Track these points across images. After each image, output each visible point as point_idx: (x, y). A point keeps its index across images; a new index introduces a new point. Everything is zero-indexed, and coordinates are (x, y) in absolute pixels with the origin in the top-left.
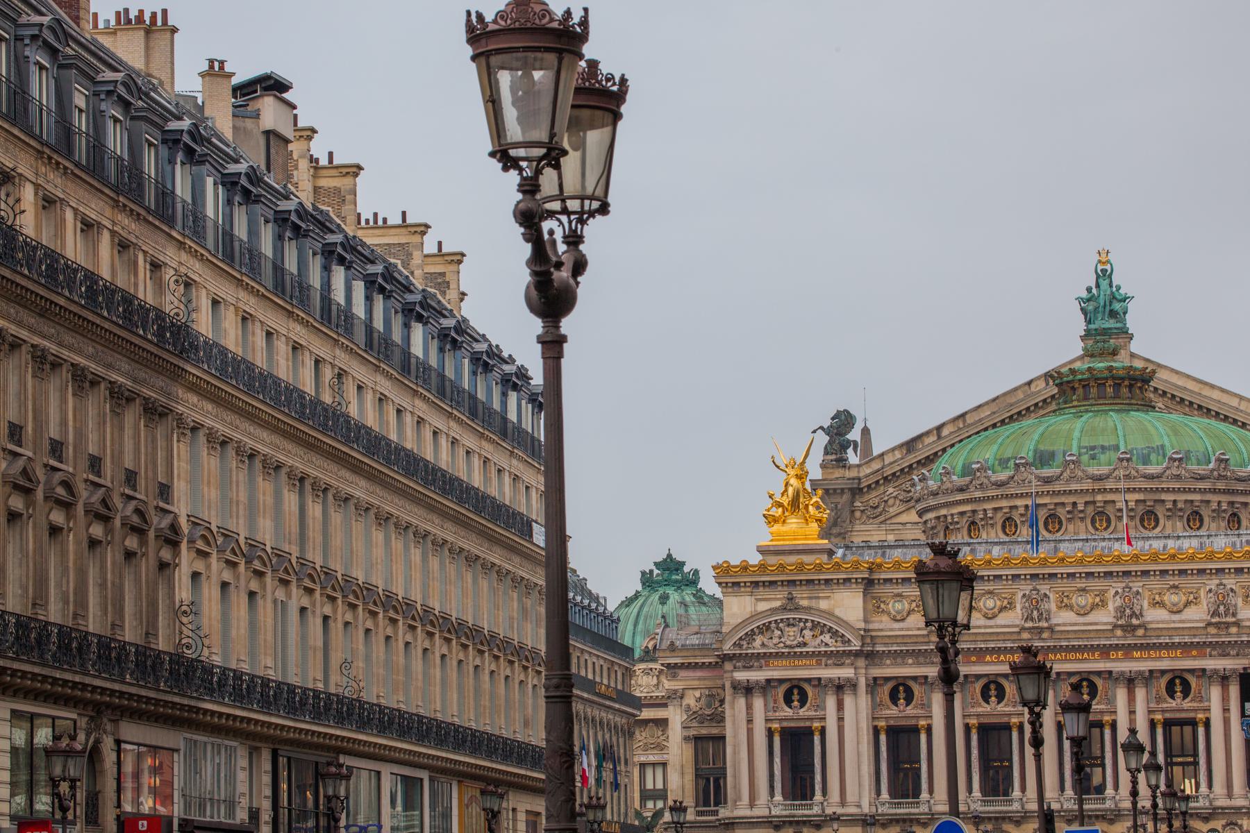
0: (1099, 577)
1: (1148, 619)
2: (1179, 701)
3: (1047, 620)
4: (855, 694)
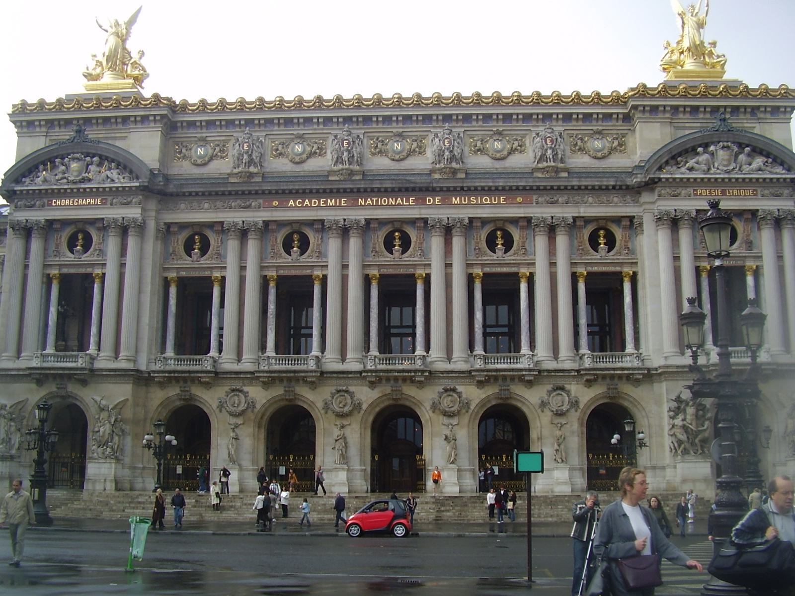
0: (417, 121)
1: (469, 166)
3: (360, 164)
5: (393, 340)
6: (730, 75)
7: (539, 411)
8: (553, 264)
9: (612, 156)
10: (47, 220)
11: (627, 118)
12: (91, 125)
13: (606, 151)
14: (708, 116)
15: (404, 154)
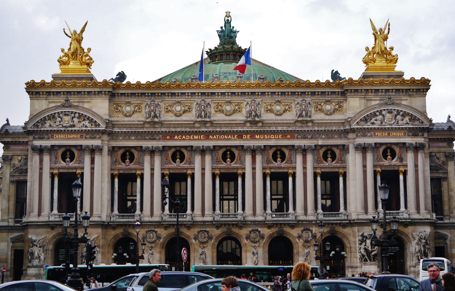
0: (238, 95)
2: (279, 163)
3: (209, 117)
4: (101, 155)
5: (224, 201)
6: (398, 68)
7: (297, 240)
8: (305, 168)
9: (335, 113)
10: (51, 145)
11: (343, 94)
12: (71, 95)
13: (332, 111)
14: (383, 94)
15: (232, 112)
